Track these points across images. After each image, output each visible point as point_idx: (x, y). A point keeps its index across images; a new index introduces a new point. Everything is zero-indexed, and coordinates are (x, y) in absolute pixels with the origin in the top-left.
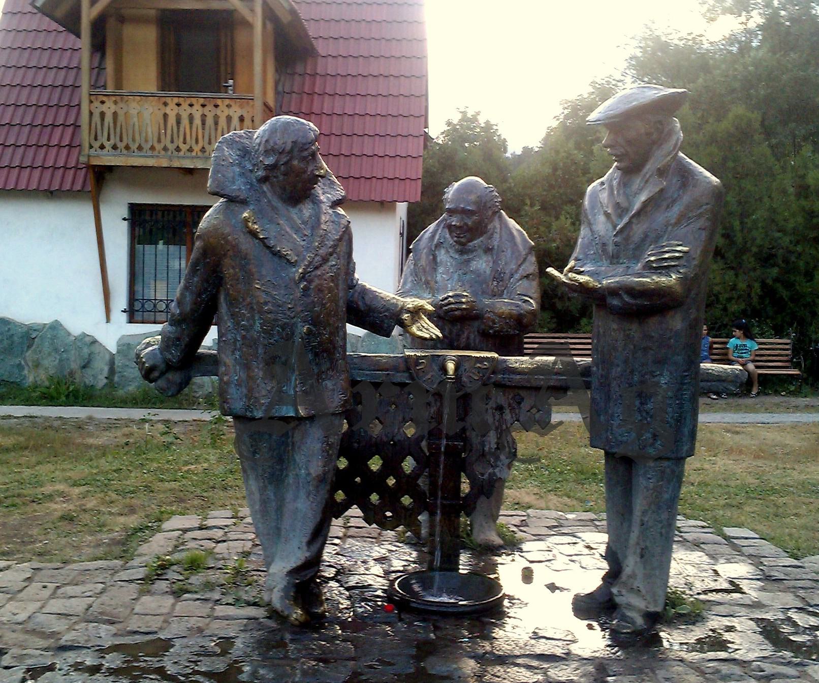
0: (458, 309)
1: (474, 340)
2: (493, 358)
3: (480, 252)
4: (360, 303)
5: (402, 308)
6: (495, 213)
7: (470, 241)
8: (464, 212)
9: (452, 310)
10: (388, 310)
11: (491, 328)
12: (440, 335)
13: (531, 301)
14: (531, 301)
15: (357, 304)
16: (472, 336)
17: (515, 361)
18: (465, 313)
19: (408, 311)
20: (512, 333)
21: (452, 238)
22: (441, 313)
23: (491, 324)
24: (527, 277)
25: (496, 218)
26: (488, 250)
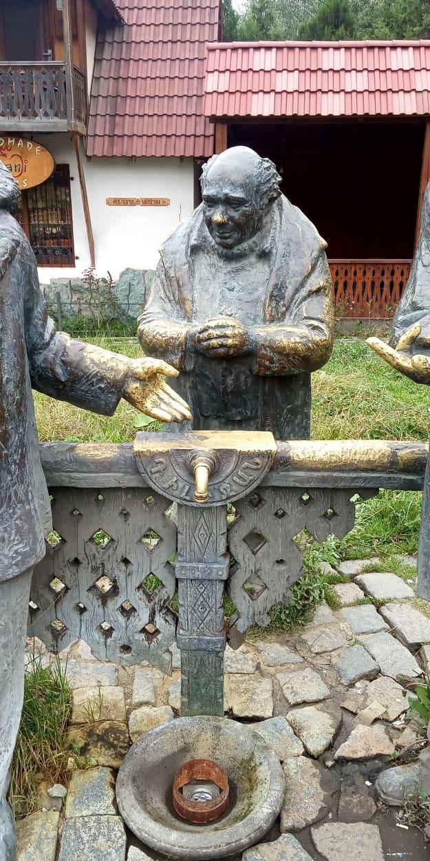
0: (222, 346)
1: (246, 382)
2: (267, 455)
3: (253, 259)
4: (59, 370)
5: (126, 375)
6: (272, 200)
7: (240, 241)
8: (229, 202)
9: (214, 348)
10: (102, 379)
11: (268, 368)
12: (188, 414)
13: (323, 326)
14: (323, 326)
15: (53, 371)
16: (243, 378)
17: (299, 449)
18: (231, 351)
19: (137, 378)
20: (296, 372)
21: (214, 238)
22: (199, 347)
23: (267, 363)
24: (318, 291)
25: (275, 205)
26: (264, 255)
